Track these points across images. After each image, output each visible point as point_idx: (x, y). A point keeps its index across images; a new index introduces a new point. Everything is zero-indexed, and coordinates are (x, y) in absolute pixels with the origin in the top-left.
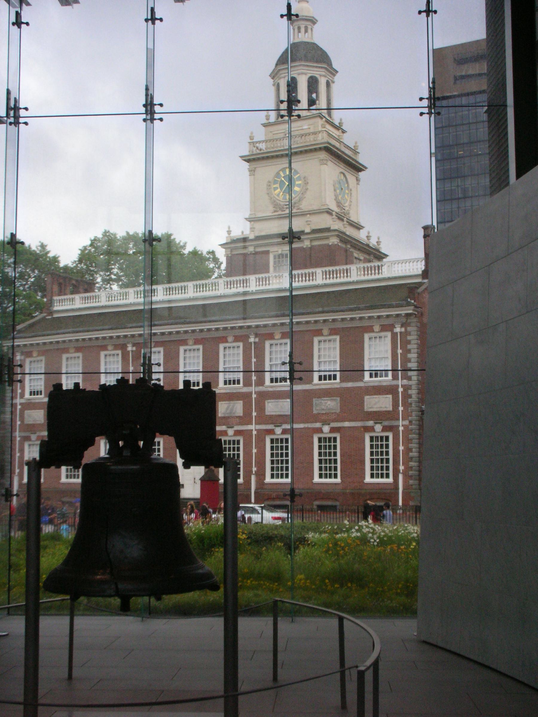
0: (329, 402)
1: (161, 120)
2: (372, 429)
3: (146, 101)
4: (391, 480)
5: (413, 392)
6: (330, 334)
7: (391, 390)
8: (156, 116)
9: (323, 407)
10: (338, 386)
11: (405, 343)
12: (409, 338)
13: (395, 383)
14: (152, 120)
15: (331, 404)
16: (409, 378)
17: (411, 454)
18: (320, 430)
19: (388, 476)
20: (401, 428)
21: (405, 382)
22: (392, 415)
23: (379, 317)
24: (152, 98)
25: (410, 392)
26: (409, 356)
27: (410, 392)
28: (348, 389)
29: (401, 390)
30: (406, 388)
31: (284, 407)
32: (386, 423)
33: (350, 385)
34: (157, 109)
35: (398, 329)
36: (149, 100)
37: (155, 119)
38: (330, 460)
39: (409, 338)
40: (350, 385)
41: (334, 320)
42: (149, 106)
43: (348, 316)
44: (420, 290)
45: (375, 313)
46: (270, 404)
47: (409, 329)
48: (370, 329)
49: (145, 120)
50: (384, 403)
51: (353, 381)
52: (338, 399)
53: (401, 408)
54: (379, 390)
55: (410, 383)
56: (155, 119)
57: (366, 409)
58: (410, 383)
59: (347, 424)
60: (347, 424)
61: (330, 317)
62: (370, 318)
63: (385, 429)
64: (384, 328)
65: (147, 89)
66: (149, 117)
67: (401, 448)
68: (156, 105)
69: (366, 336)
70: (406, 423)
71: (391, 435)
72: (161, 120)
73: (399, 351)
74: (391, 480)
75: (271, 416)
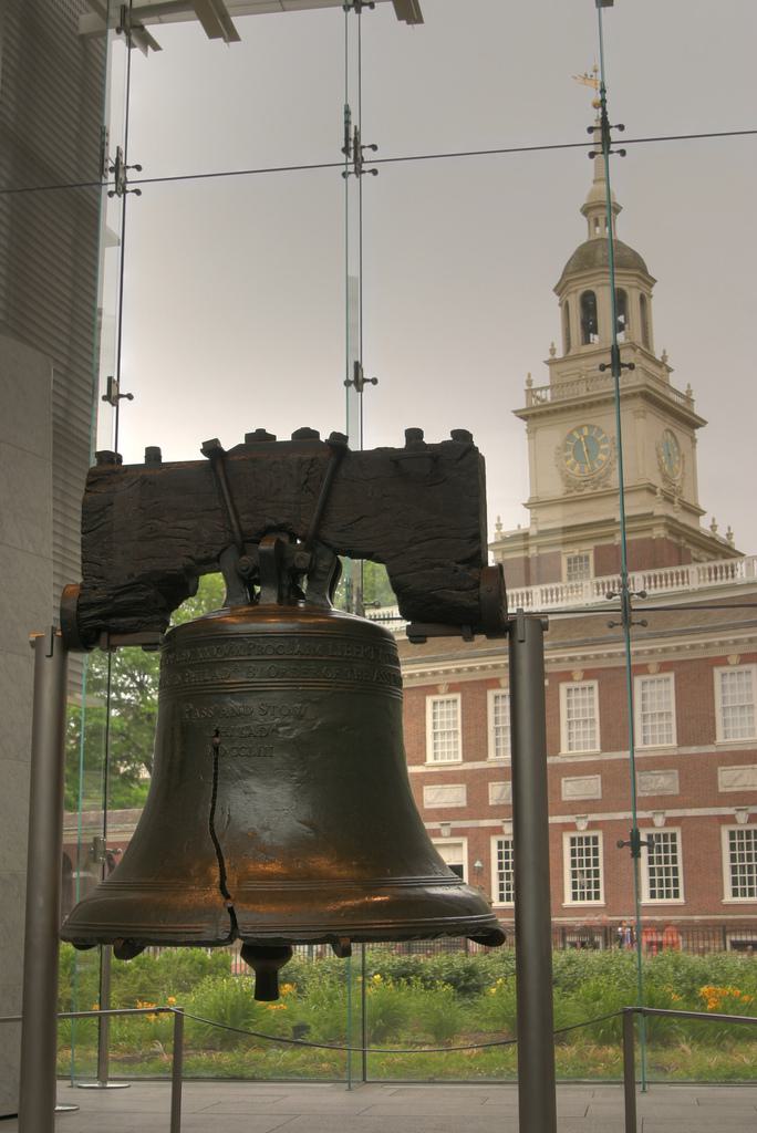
0: (662, 779)
2: (731, 820)
3: (347, 139)
6: (660, 671)
8: (365, 167)
9: (653, 786)
10: (676, 753)
14: (359, 172)
15: (666, 782)
18: (649, 823)
24: (357, 134)
28: (691, 756)
31: (590, 787)
33: (693, 750)
34: (367, 154)
36: (352, 136)
37: (364, 172)
38: (667, 869)
40: (693, 750)
41: (665, 650)
42: (352, 146)
43: (687, 642)
45: (730, 637)
46: (569, 784)
48: (723, 661)
49: (345, 175)
51: (698, 744)
52: (676, 771)
56: (364, 172)
57: (721, 790)
61: (659, 645)
62: (722, 644)
65: (347, 112)
66: (351, 168)
68: (364, 147)
69: (717, 672)
72: (375, 172)
75: (571, 803)
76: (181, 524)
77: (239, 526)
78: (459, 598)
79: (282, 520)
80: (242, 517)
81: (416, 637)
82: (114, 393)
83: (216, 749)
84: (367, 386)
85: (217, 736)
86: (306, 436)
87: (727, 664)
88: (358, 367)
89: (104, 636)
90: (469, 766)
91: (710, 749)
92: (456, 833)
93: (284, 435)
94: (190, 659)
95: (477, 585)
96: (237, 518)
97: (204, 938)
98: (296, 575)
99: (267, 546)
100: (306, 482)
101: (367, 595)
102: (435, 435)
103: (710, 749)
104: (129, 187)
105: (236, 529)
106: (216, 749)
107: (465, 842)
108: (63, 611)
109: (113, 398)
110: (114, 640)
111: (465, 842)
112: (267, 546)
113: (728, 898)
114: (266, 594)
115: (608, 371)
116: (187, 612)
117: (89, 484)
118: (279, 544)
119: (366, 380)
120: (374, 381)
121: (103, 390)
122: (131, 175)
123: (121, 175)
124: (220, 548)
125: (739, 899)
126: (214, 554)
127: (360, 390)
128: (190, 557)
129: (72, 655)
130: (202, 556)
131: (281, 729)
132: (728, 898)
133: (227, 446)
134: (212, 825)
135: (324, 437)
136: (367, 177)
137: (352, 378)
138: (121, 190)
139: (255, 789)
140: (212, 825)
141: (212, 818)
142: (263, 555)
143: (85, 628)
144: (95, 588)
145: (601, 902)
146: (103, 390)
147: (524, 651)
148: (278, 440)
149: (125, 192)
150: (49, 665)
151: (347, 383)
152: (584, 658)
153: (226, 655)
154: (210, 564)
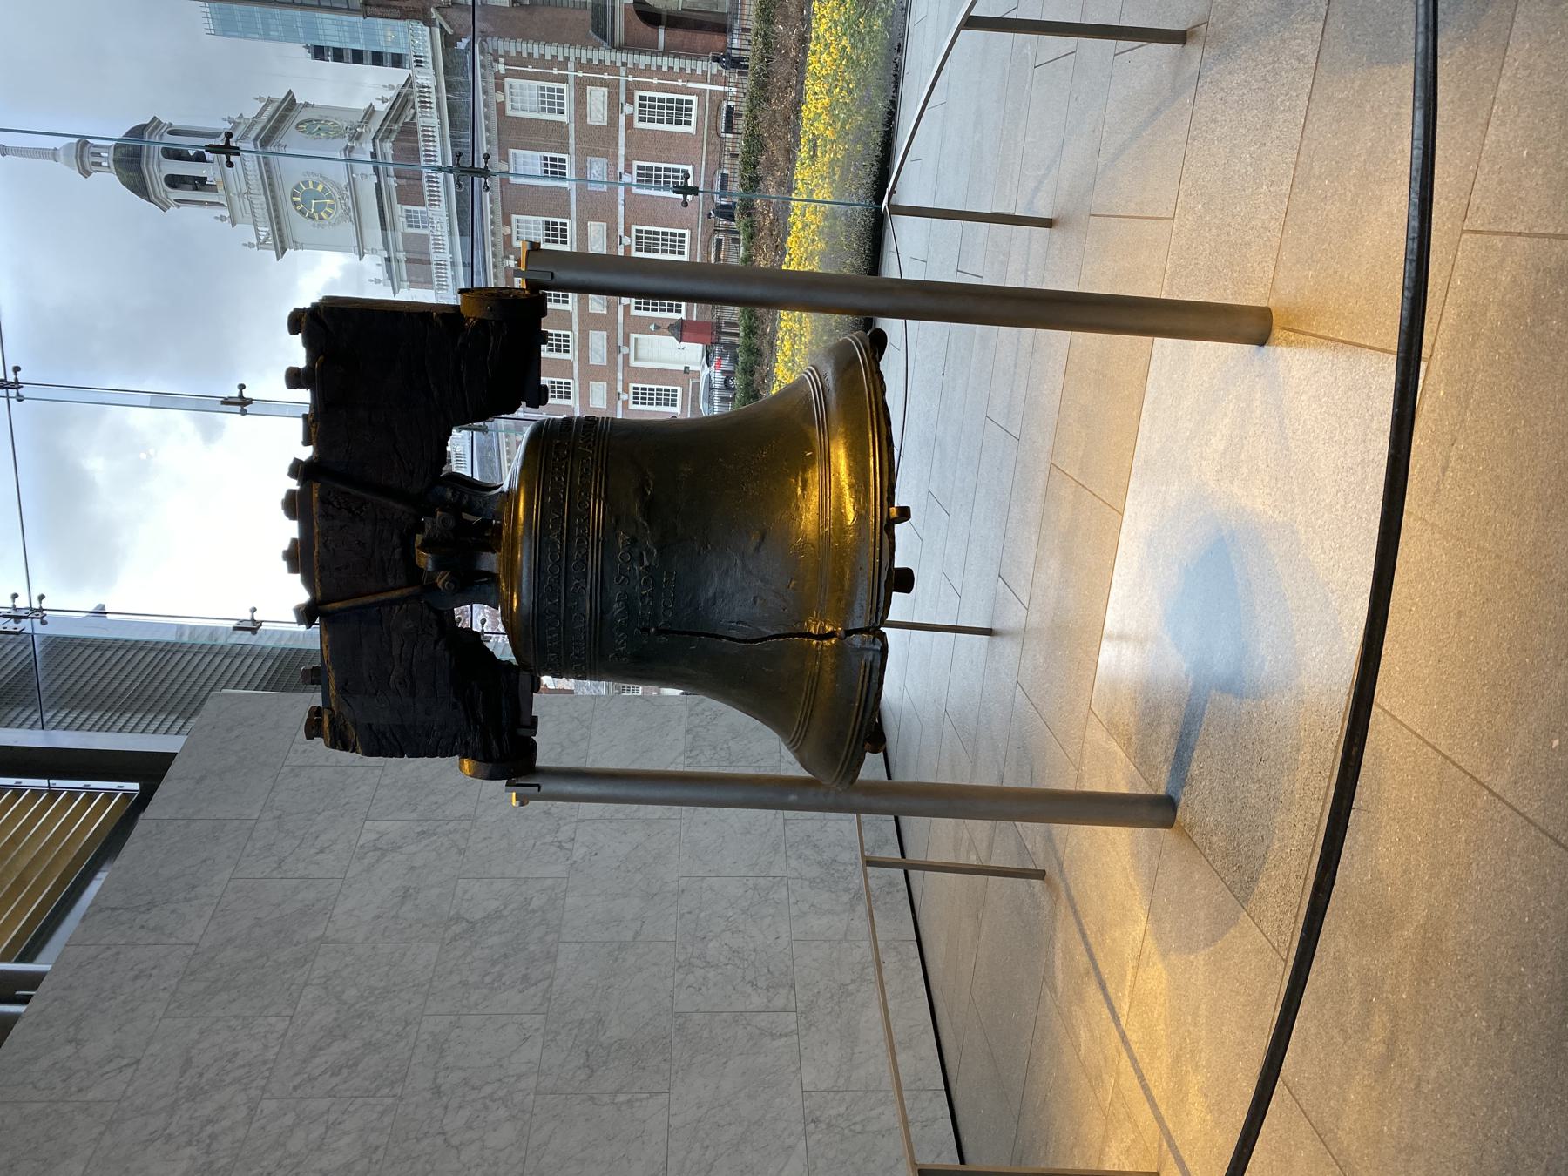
1: (16, 369)
2: (630, 118)
4: (694, 98)
5: (585, 54)
7: (581, 87)
8: (11, 378)
11: (520, 60)
12: (513, 54)
13: (571, 81)
16: (567, 59)
17: (665, 69)
18: (628, 186)
19: (689, 102)
20: (631, 79)
21: (571, 65)
22: (613, 87)
23: (485, 92)
25: (584, 61)
26: (536, 56)
27: (584, 61)
29: (580, 74)
30: (579, 65)
32: (623, 98)
35: (502, 68)
39: (513, 54)
44: (450, 32)
47: (501, 52)
48: (501, 107)
50: (597, 99)
53: (606, 76)
54: (581, 101)
55: (572, 59)
58: (572, 59)
59: (622, 151)
60: (622, 151)
63: (630, 100)
64: (500, 88)
67: (655, 81)
69: (510, 113)
70: (623, 71)
71: (638, 93)
73: (530, 69)
74: (694, 98)
76: (396, 652)
77: (400, 588)
78: (491, 347)
79: (396, 540)
80: (390, 582)
81: (539, 397)
82: (250, 625)
83: (660, 632)
84: (246, 394)
85: (647, 630)
86: (293, 505)
87: (503, 103)
88: (227, 402)
89: (523, 732)
90: (575, 326)
91: (572, 127)
92: (627, 342)
93: (291, 530)
94: (554, 642)
95: (482, 323)
96: (393, 589)
97: (878, 664)
98: (464, 526)
99: (425, 561)
100: (349, 510)
101: (487, 453)
102: (296, 353)
103: (572, 127)
104: (36, 605)
105: (405, 591)
106: (660, 632)
107: (633, 336)
108: (492, 777)
109: (254, 627)
110: (525, 720)
111: (633, 336)
112: (425, 561)
113: (691, 129)
114: (490, 562)
115: (233, 158)
116: (500, 646)
117: (345, 749)
118: (425, 546)
119: (241, 396)
120: (242, 387)
121: (246, 638)
122: (22, 603)
123: (23, 614)
124: (426, 611)
125: (693, 120)
126: (432, 616)
127: (250, 401)
128: (436, 643)
129: (538, 764)
130: (435, 631)
131: (646, 563)
132: (691, 129)
133: (303, 596)
134: (745, 641)
135: (294, 484)
136: (21, 377)
137: (238, 408)
138: (38, 614)
139: (711, 594)
140: (745, 641)
141: (739, 641)
142: (439, 566)
143: (508, 752)
144: (467, 744)
145: (687, 232)
146: (246, 638)
147: (563, 276)
148: (296, 536)
149: (41, 610)
150: (549, 786)
151: (244, 412)
152: (493, 223)
153: (558, 617)
154: (447, 624)
